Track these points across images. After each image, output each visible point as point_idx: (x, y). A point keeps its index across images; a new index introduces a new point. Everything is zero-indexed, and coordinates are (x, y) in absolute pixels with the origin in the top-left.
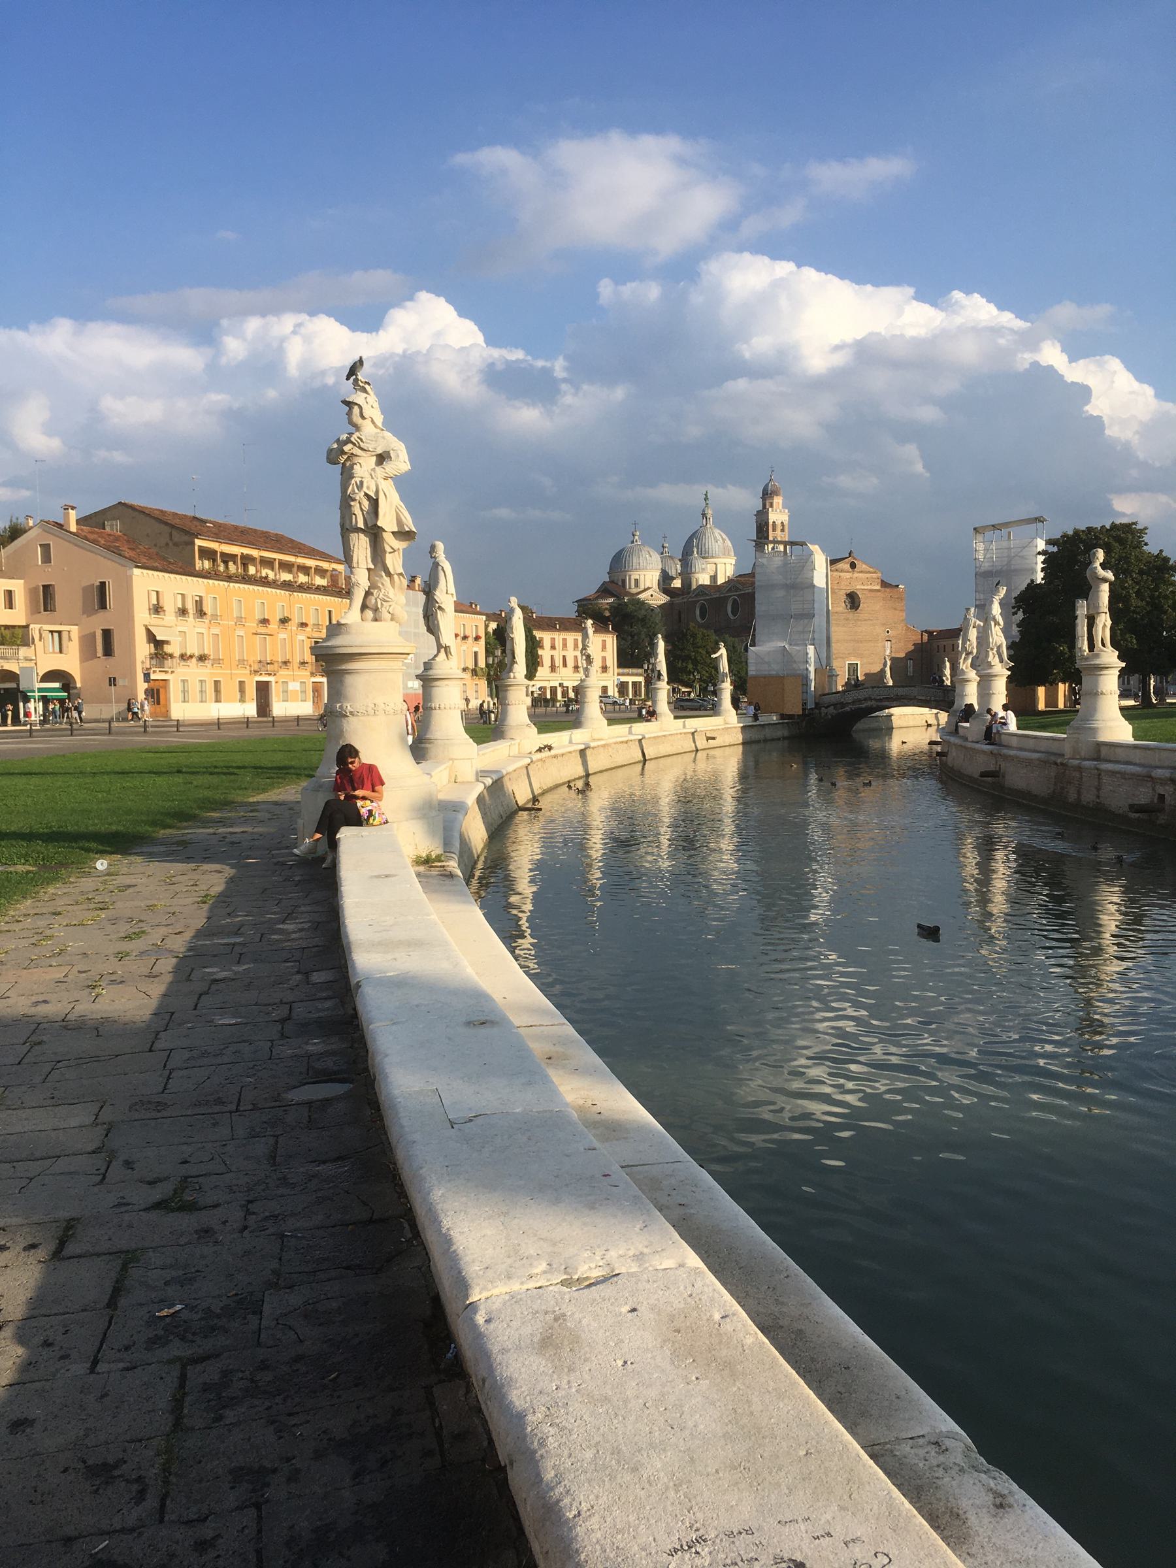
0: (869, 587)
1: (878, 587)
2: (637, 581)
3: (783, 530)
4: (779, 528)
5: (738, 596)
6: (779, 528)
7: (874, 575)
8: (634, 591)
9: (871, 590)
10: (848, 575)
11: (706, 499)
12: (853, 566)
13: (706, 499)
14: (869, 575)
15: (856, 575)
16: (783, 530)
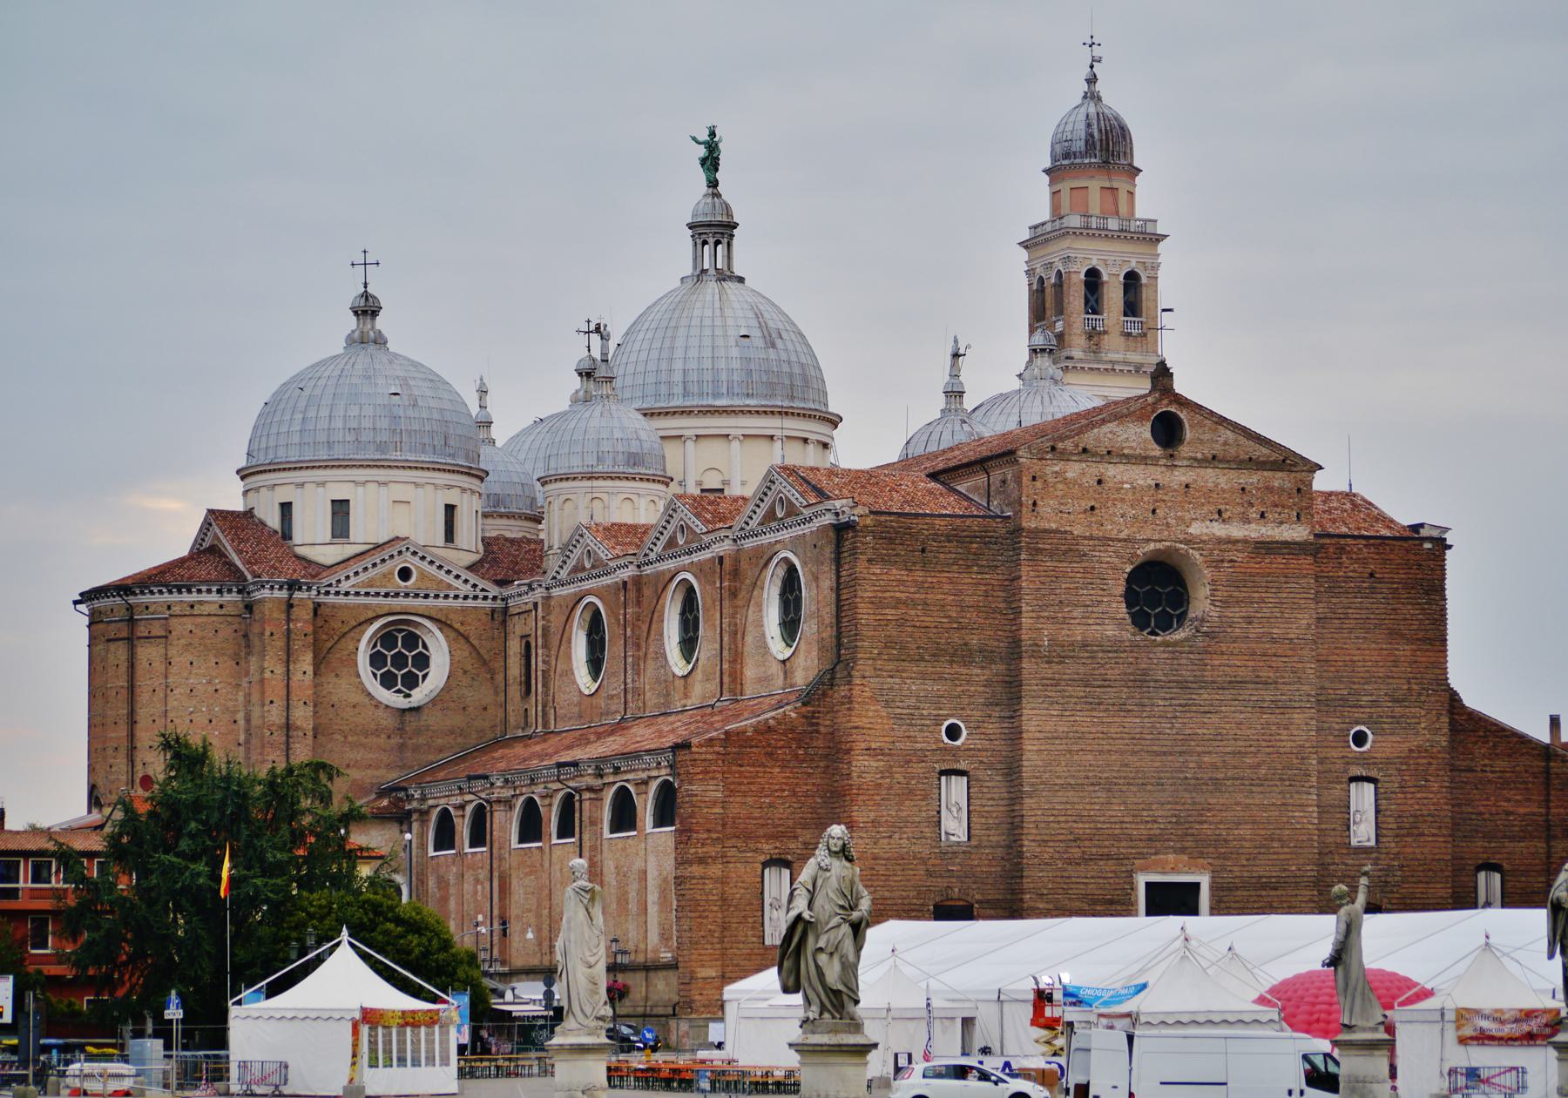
0: (1256, 531)
1: (1298, 533)
2: (341, 509)
3: (1132, 307)
4: (1114, 296)
5: (699, 569)
6: (1114, 296)
7: (1279, 479)
8: (328, 554)
9: (1265, 548)
10: (1142, 476)
11: (711, 162)
12: (1168, 430)
13: (711, 162)
14: (1253, 478)
15: (1180, 476)
16: (1132, 307)
